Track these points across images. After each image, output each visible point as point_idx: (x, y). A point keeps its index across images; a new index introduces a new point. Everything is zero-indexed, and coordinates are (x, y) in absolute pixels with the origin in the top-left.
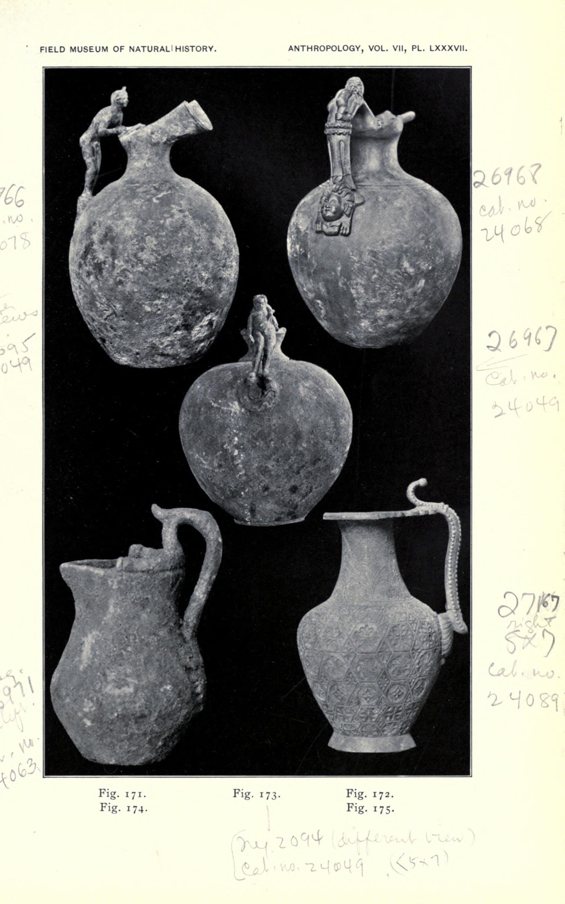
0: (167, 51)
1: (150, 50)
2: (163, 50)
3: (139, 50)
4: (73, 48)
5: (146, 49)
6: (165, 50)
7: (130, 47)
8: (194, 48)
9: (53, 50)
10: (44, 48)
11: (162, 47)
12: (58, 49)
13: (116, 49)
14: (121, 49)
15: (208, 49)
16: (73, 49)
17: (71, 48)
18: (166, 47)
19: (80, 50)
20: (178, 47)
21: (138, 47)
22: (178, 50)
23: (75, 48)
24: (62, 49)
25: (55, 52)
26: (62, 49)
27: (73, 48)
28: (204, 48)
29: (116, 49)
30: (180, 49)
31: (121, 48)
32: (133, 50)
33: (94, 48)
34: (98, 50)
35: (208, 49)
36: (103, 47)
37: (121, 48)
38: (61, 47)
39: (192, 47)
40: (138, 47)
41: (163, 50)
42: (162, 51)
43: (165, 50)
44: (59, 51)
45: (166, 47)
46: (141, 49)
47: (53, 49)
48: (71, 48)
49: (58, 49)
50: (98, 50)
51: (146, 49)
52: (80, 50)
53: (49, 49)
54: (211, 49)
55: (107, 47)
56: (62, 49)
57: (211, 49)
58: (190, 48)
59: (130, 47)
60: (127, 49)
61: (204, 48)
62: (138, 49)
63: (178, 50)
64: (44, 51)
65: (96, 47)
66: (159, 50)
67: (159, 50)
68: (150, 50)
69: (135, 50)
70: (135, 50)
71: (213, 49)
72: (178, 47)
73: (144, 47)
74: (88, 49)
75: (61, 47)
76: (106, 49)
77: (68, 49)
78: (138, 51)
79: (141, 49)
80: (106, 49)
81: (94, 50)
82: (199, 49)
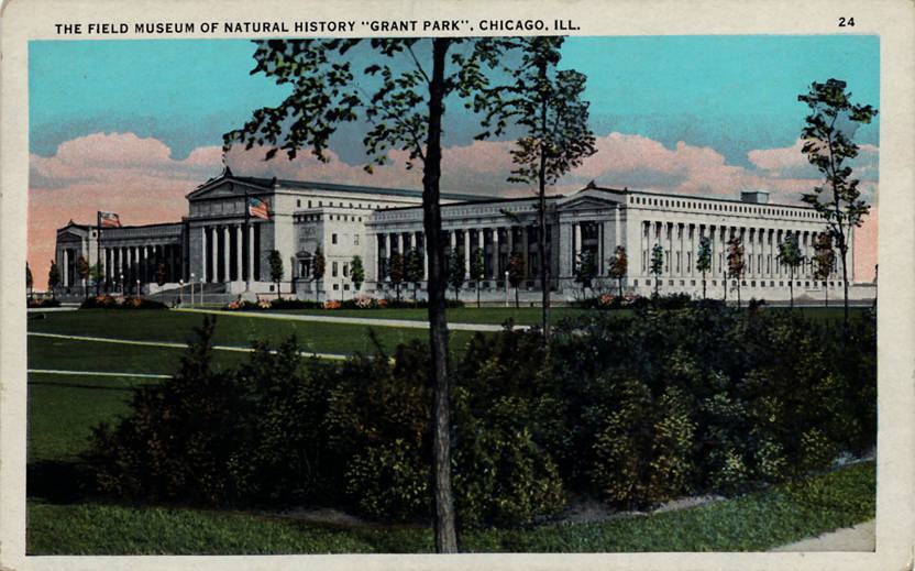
0: (283, 30)
9: (109, 29)
12: (117, 28)
13: (205, 28)
14: (213, 28)
16: (139, 28)
24: (124, 28)
26: (124, 28)
29: (205, 28)
31: (214, 26)
36: (187, 25)
37: (214, 26)
46: (244, 27)
48: (137, 26)
49: (117, 28)
51: (250, 27)
55: (192, 25)
56: (124, 28)
59: (226, 25)
60: (221, 27)
62: (239, 27)
74: (164, 27)
76: (190, 27)
77: (132, 28)
79: (244, 27)
80: (190, 27)
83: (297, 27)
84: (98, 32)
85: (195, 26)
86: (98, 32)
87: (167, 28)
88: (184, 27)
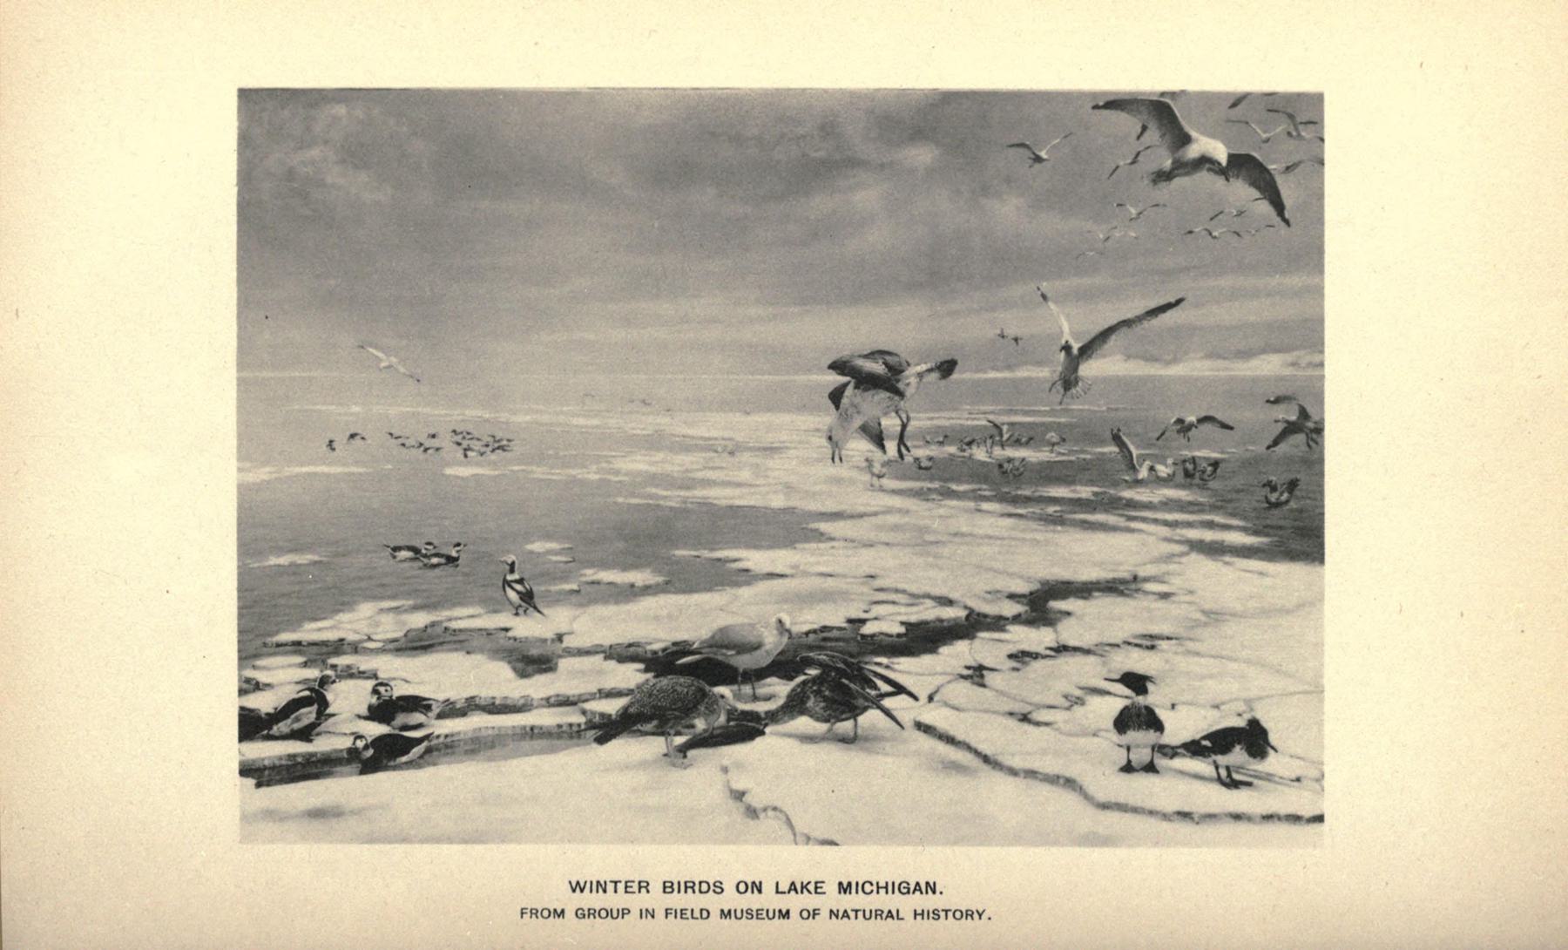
0: (898, 918)
1: (868, 916)
2: (892, 917)
3: (848, 917)
4: (726, 912)
5: (860, 914)
6: (895, 914)
7: (831, 911)
8: (950, 914)
10: (673, 912)
11: (890, 912)
12: (697, 914)
13: (805, 914)
14: (814, 914)
15: (976, 916)
17: (722, 911)
18: (898, 911)
19: (739, 915)
20: (919, 911)
21: (845, 911)
22: (919, 918)
23: (729, 911)
25: (693, 918)
27: (726, 912)
28: (969, 914)
30: (922, 914)
32: (837, 917)
33: (764, 913)
34: (771, 915)
35: (976, 916)
36: (780, 911)
38: (701, 910)
39: (946, 911)
40: (845, 911)
41: (892, 917)
42: (889, 920)
43: (896, 918)
44: (699, 916)
45: (898, 911)
46: (852, 915)
47: (689, 913)
48: (722, 911)
49: (697, 914)
50: (771, 915)
51: (860, 914)
52: (739, 915)
53: (682, 914)
54: (980, 915)
57: (980, 915)
58: (942, 914)
61: (969, 914)
63: (919, 918)
64: (671, 917)
65: (768, 911)
66: (884, 916)
67: (884, 916)
68: (868, 916)
69: (840, 915)
70: (840, 915)
71: (983, 917)
72: (919, 911)
73: (856, 911)
74: (754, 913)
75: (701, 910)
78: (845, 919)
79: (852, 915)
81: (764, 915)
82: (958, 915)
83: (916, 914)
84: (676, 917)
85: (791, 915)
86: (676, 917)
87: (757, 915)
88: (777, 913)
